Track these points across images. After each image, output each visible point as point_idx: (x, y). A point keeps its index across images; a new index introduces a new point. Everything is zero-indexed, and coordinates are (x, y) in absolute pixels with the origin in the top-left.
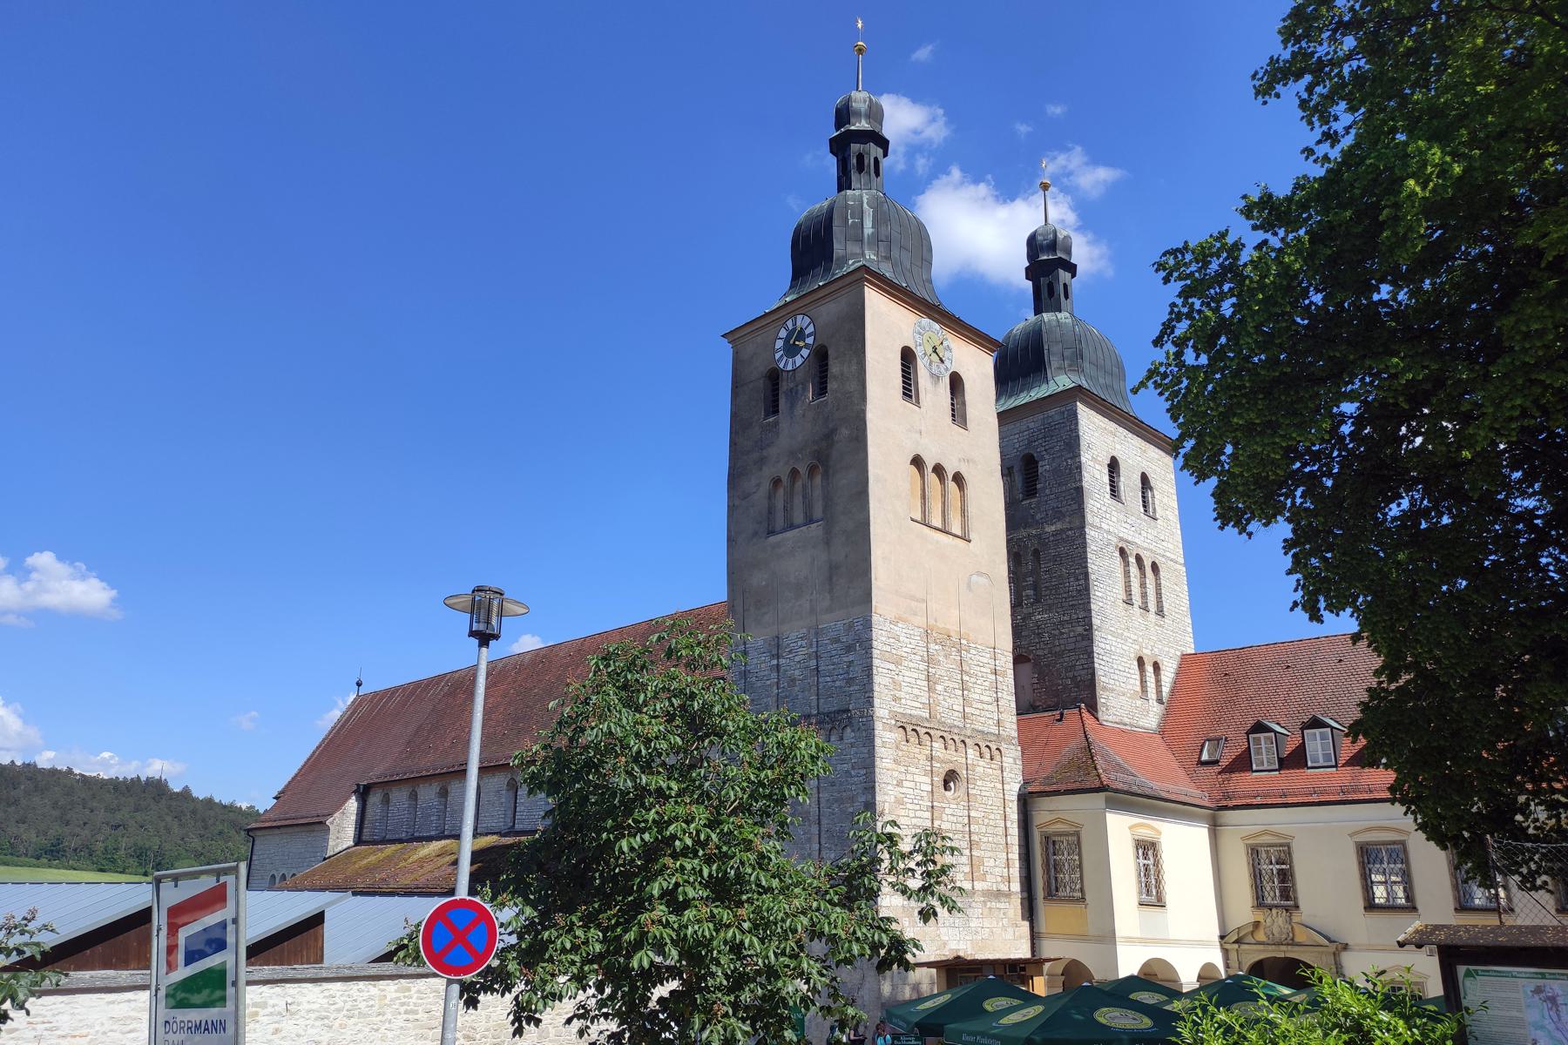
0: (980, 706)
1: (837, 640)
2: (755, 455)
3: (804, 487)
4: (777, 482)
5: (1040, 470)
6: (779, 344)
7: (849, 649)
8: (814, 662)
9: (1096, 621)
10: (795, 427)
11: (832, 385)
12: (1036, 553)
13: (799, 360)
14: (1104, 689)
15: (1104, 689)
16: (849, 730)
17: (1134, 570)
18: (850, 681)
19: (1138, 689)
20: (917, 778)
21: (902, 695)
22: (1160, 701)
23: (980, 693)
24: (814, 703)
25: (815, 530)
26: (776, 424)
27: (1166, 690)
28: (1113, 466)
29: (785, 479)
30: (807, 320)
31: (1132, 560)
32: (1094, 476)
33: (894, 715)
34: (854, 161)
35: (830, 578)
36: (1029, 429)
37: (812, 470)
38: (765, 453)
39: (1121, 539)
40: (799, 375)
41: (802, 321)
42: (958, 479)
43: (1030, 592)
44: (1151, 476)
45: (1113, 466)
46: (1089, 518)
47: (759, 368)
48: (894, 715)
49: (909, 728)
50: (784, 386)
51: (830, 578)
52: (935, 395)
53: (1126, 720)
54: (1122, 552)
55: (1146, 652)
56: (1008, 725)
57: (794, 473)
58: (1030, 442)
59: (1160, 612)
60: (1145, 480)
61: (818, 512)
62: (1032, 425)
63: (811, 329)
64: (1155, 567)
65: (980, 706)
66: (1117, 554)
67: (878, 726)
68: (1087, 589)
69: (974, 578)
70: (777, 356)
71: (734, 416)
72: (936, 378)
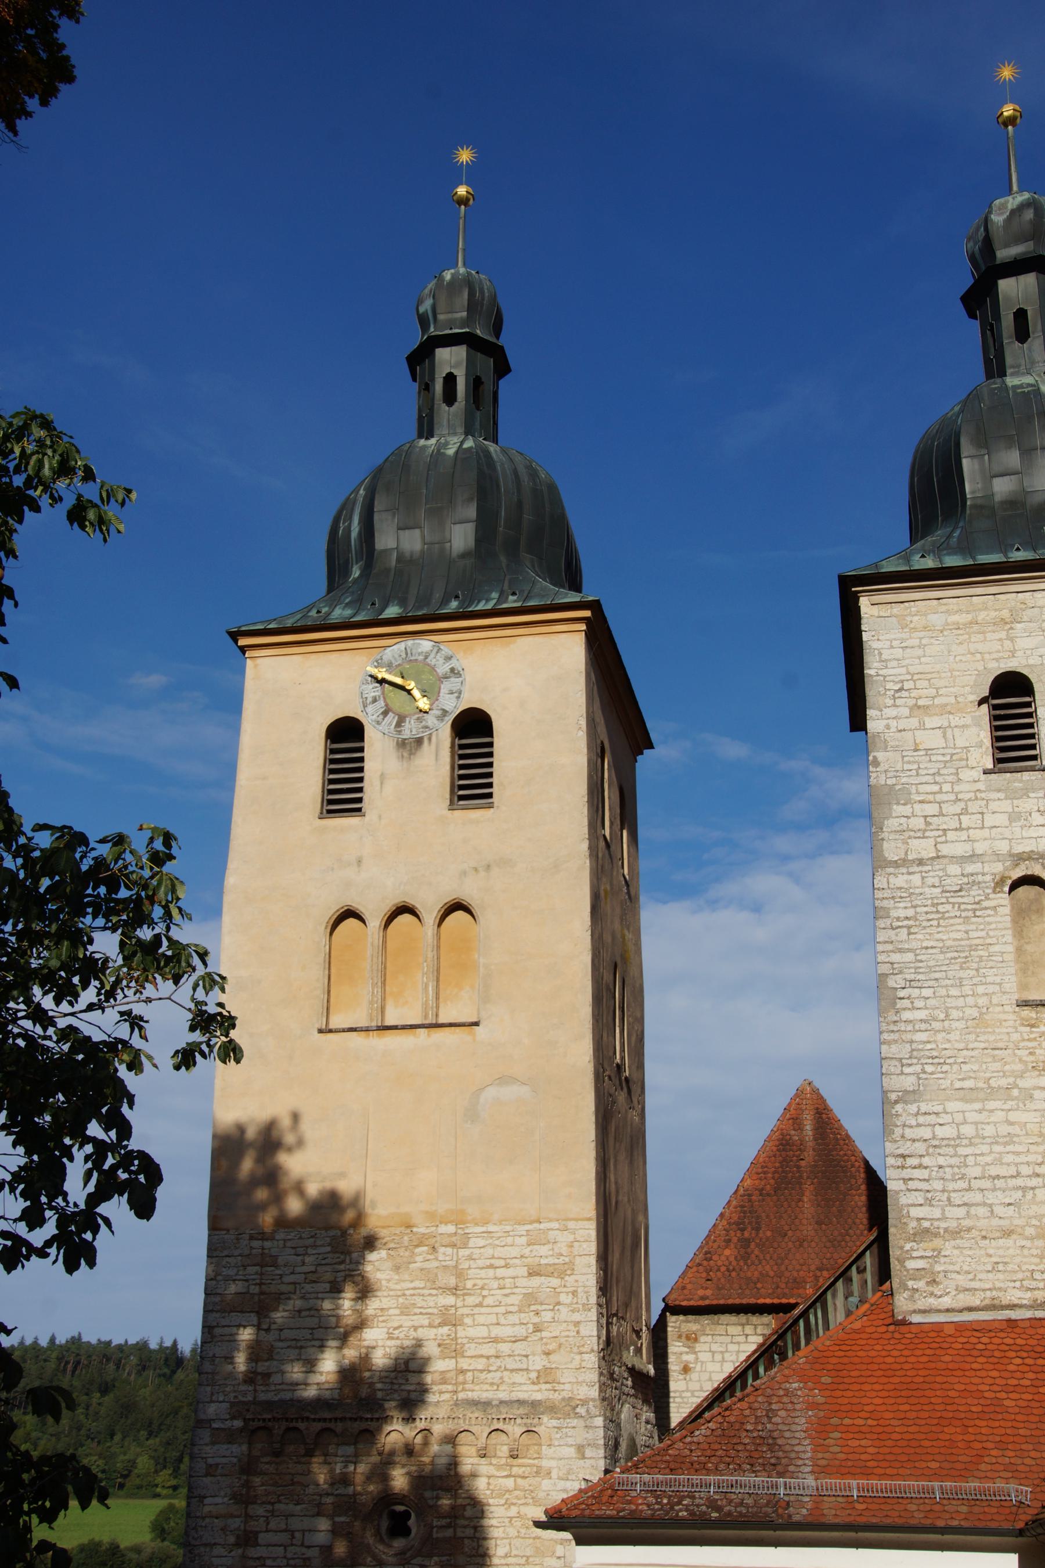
14: (923, 1234)
15: (923, 1234)
20: (296, 1524)
33: (238, 1409)
34: (439, 387)
39: (1020, 858)
53: (1014, 1296)
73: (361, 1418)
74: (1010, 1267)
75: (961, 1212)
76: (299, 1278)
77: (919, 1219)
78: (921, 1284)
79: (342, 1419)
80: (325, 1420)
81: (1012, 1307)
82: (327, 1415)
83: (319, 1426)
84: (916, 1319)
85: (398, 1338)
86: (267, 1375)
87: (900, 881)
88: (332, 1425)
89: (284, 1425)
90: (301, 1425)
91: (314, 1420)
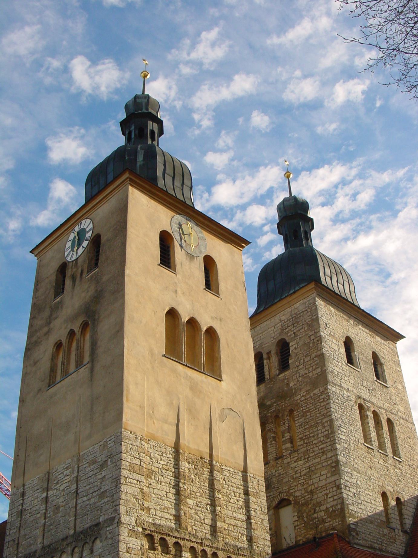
0: (232, 522)
1: (94, 462)
2: (46, 329)
3: (78, 342)
4: (59, 345)
5: (291, 349)
6: (69, 244)
7: (103, 465)
8: (74, 486)
9: (342, 458)
10: (75, 299)
11: (102, 258)
12: (291, 411)
13: (81, 250)
16: (98, 541)
17: (371, 423)
18: (102, 495)
19: (384, 519)
21: (152, 505)
22: (405, 532)
23: (231, 513)
24: (72, 524)
25: (84, 372)
26: (61, 302)
27: (408, 522)
28: (348, 344)
29: (64, 341)
30: (89, 221)
31: (370, 414)
32: (334, 349)
33: (139, 522)
35: (92, 408)
36: (281, 321)
37: (85, 326)
38: (52, 326)
40: (80, 261)
41: (87, 224)
42: (211, 331)
43: (289, 445)
44: (381, 355)
45: (348, 344)
46: (330, 377)
47: (55, 266)
48: (139, 522)
49: (157, 537)
50: (69, 273)
51: (92, 408)
52: (190, 270)
53: (376, 546)
54: (361, 407)
55: (389, 489)
56: (261, 542)
57: (72, 333)
58: (282, 330)
59: (396, 452)
60: (375, 356)
61: (87, 359)
62: (283, 318)
63: (91, 226)
64: (390, 422)
65: (232, 522)
66: (356, 408)
67: (124, 532)
68: (333, 432)
69: (227, 411)
70: (66, 254)
71: (34, 305)
72: (191, 257)
73: (190, 541)
74: (373, 535)
75: (360, 510)
76: (161, 466)
77: (352, 510)
78: (354, 534)
79: (183, 539)
80: (176, 537)
81: (375, 549)
82: (178, 535)
83: (175, 540)
84: (356, 546)
85: (200, 507)
86: (149, 509)
87: (334, 389)
88: (179, 541)
89: (160, 536)
90: (167, 538)
91: (171, 536)
